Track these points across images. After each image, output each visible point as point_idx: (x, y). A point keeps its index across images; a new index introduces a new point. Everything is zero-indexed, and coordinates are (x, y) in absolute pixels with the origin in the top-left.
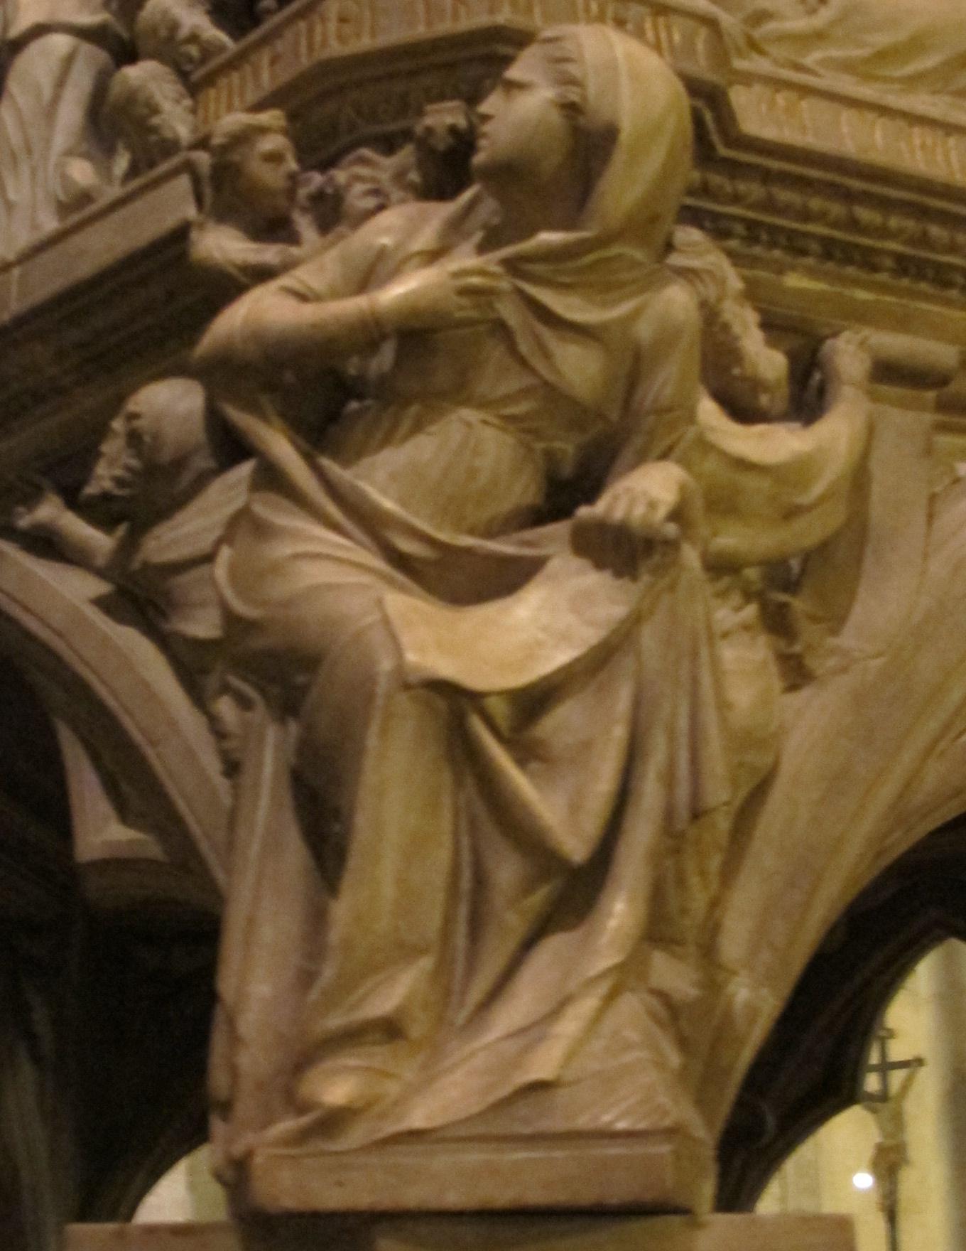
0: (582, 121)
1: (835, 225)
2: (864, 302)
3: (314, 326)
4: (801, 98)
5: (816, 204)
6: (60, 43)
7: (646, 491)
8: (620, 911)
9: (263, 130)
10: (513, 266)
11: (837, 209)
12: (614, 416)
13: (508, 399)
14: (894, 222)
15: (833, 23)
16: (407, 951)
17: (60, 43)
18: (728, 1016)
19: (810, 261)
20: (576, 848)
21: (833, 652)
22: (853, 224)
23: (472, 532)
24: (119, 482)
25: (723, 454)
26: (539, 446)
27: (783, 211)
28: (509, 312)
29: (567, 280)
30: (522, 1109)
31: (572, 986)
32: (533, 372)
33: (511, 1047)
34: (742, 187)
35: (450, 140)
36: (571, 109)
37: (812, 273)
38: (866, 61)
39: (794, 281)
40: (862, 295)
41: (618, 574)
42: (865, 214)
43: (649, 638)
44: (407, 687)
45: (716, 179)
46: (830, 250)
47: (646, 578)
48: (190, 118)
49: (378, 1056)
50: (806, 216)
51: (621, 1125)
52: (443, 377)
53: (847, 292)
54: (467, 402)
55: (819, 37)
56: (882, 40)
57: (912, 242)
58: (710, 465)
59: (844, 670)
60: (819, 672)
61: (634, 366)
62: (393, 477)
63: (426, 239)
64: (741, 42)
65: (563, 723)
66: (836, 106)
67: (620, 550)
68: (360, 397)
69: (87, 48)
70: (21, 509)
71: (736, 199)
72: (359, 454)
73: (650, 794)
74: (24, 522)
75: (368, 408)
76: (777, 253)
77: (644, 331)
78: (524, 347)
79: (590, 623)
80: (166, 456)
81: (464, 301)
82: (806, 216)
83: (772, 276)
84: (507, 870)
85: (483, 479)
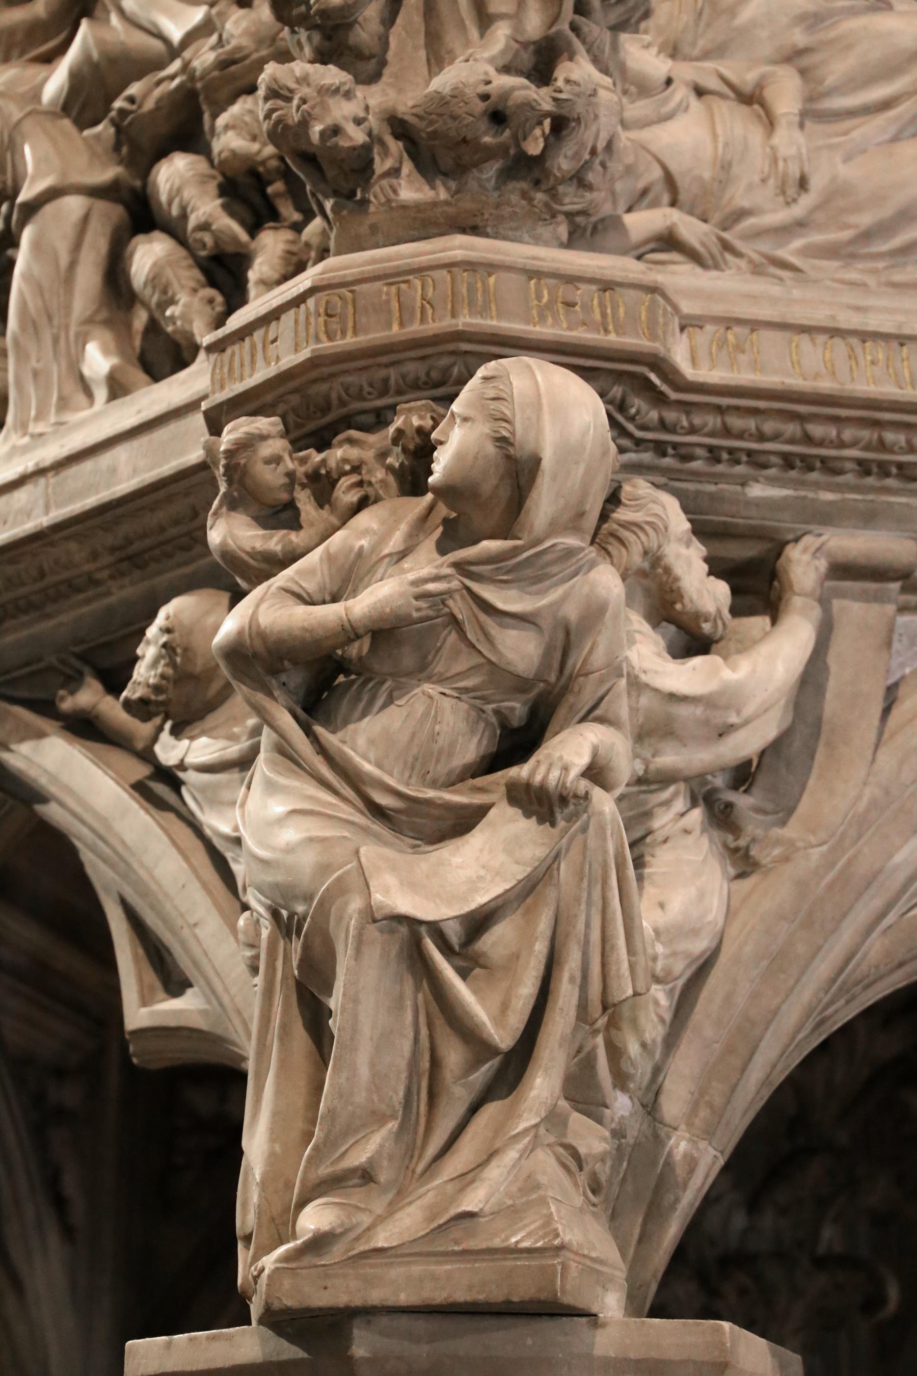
0: (512, 451)
1: (792, 441)
2: (831, 503)
3: (305, 629)
4: (753, 331)
5: (769, 427)
6: (74, 205)
7: (568, 752)
8: (543, 1085)
9: (263, 438)
10: (461, 567)
11: (791, 429)
12: (553, 678)
13: (460, 675)
14: (848, 434)
15: (817, 208)
16: (380, 1118)
17: (74, 205)
18: (669, 1164)
19: (772, 472)
20: (504, 1037)
21: (778, 842)
22: (808, 439)
23: (434, 784)
24: (157, 689)
25: (656, 690)
26: (489, 708)
27: (740, 436)
28: (459, 607)
29: (505, 578)
30: (456, 1232)
31: (498, 1144)
32: (480, 652)
33: (450, 1188)
34: (697, 420)
35: (418, 440)
36: (502, 441)
37: (772, 481)
38: (852, 242)
39: (757, 491)
40: (828, 496)
41: (541, 821)
42: (817, 430)
43: (565, 870)
44: (375, 921)
45: (671, 416)
46: (788, 461)
47: (561, 824)
48: (208, 309)
49: (357, 1196)
50: (761, 437)
51: (525, 1244)
52: (408, 660)
53: (811, 495)
54: (429, 679)
55: (801, 225)
56: (865, 220)
57: (867, 448)
58: (644, 701)
59: (786, 859)
60: (765, 861)
61: (566, 641)
62: (371, 742)
63: (395, 542)
64: (716, 249)
65: (497, 940)
66: (788, 335)
67: (541, 804)
68: (347, 673)
69: (101, 206)
70: (62, 692)
71: (693, 430)
72: (346, 723)
73: (566, 995)
74: (67, 704)
75: (354, 681)
76: (740, 469)
77: (571, 612)
78: (469, 636)
79: (517, 863)
80: (199, 665)
81: (422, 604)
82: (761, 437)
83: (739, 488)
84: (454, 1055)
85: (442, 741)
